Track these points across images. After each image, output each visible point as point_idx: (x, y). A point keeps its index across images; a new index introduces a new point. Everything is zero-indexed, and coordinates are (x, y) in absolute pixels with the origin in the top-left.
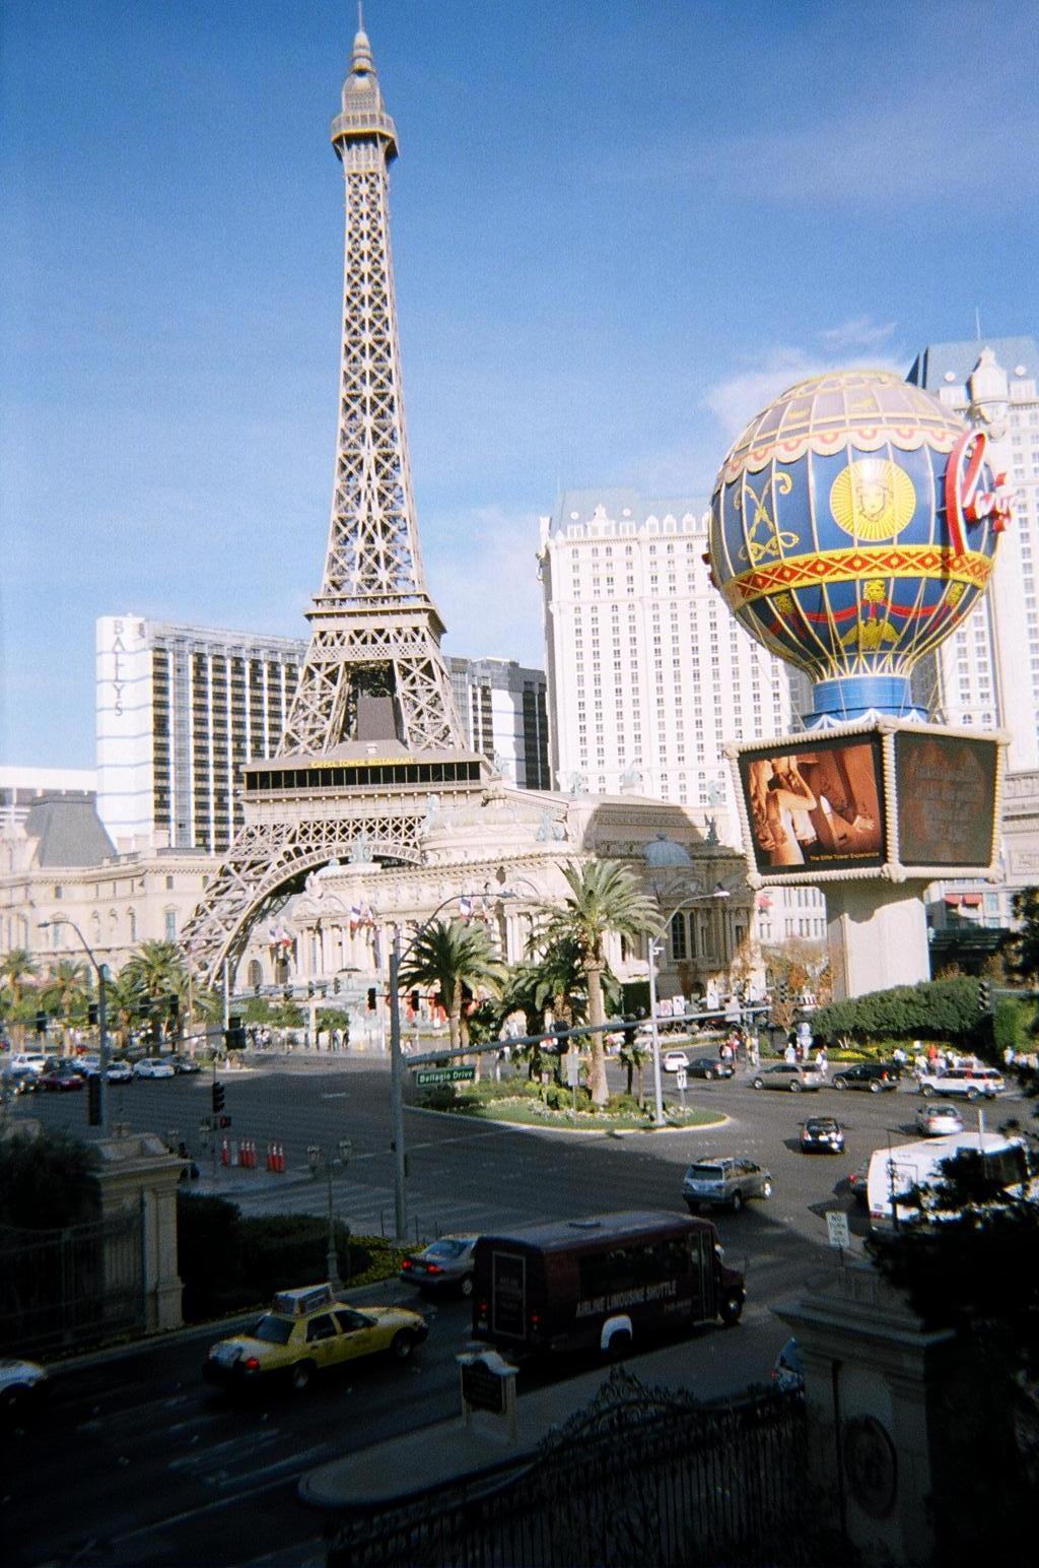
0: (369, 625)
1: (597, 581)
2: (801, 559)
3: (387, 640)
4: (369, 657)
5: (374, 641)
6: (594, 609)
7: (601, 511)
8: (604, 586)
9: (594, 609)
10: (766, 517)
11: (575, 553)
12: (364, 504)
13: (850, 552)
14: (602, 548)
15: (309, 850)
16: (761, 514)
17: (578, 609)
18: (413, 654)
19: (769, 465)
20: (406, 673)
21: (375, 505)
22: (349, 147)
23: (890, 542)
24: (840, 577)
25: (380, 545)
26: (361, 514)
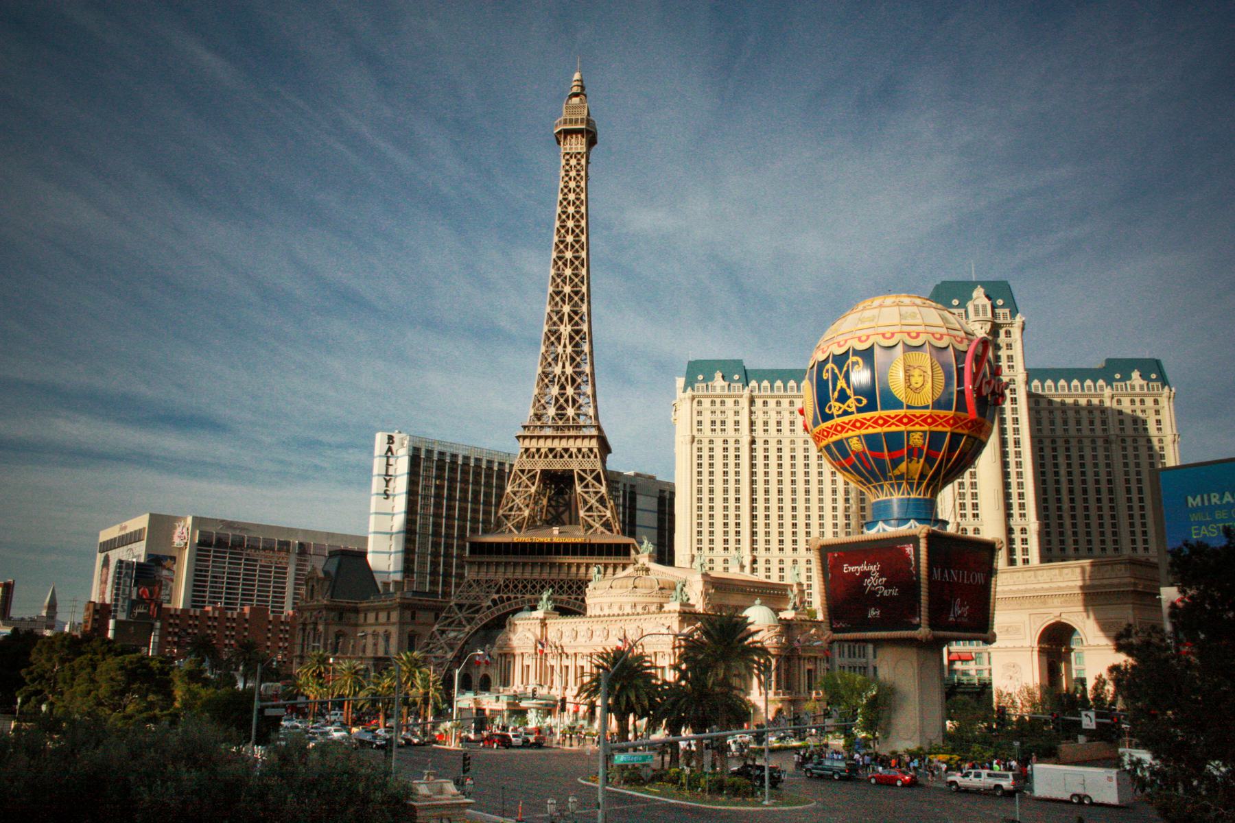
1: (713, 423)
2: (868, 415)
3: (571, 456)
4: (557, 467)
5: (562, 456)
6: (711, 442)
8: (718, 426)
9: (711, 442)
10: (845, 386)
12: (560, 364)
13: (901, 412)
14: (718, 400)
15: (509, 599)
18: (588, 467)
19: (847, 352)
20: (582, 479)
21: (567, 364)
22: (565, 138)
23: (926, 407)
24: (894, 428)
25: (570, 391)
26: (558, 370)
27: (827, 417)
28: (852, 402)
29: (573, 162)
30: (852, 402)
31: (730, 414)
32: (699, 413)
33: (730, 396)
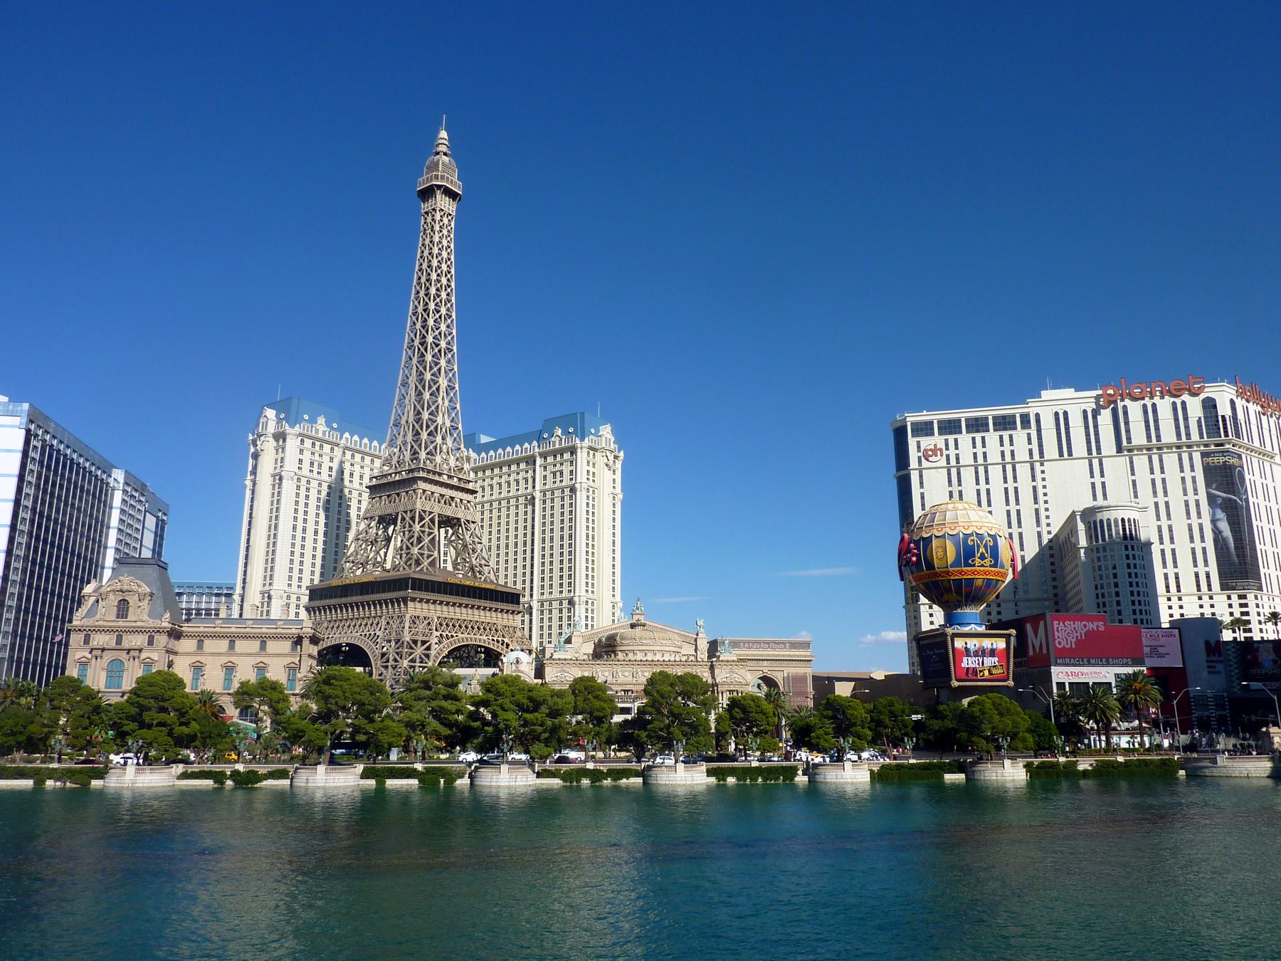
0: (449, 493)
1: (312, 464)
4: (449, 514)
6: (308, 482)
7: (321, 420)
8: (315, 469)
9: (308, 482)
11: (302, 441)
16: (982, 550)
17: (299, 480)
25: (449, 441)
27: (967, 565)
28: (988, 561)
29: (445, 220)
30: (988, 561)
31: (326, 459)
32: (301, 451)
33: (328, 442)
